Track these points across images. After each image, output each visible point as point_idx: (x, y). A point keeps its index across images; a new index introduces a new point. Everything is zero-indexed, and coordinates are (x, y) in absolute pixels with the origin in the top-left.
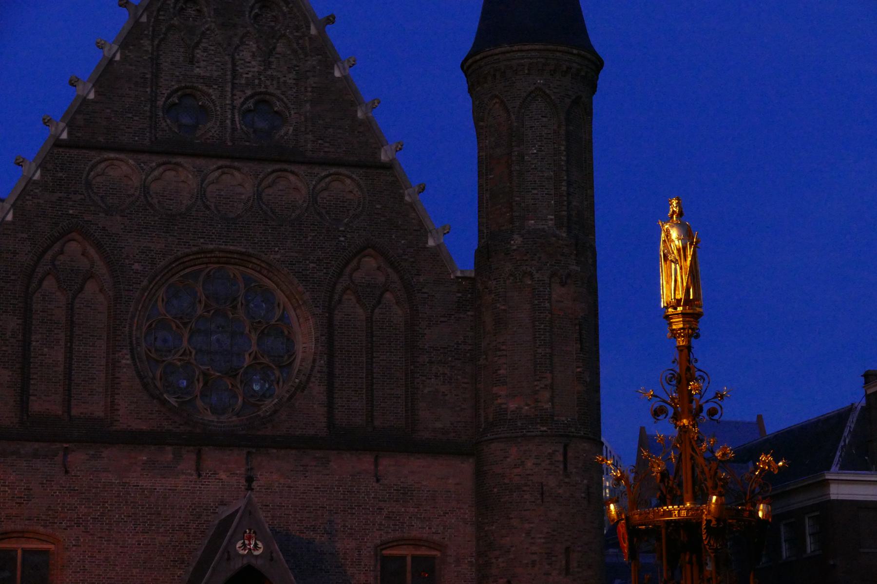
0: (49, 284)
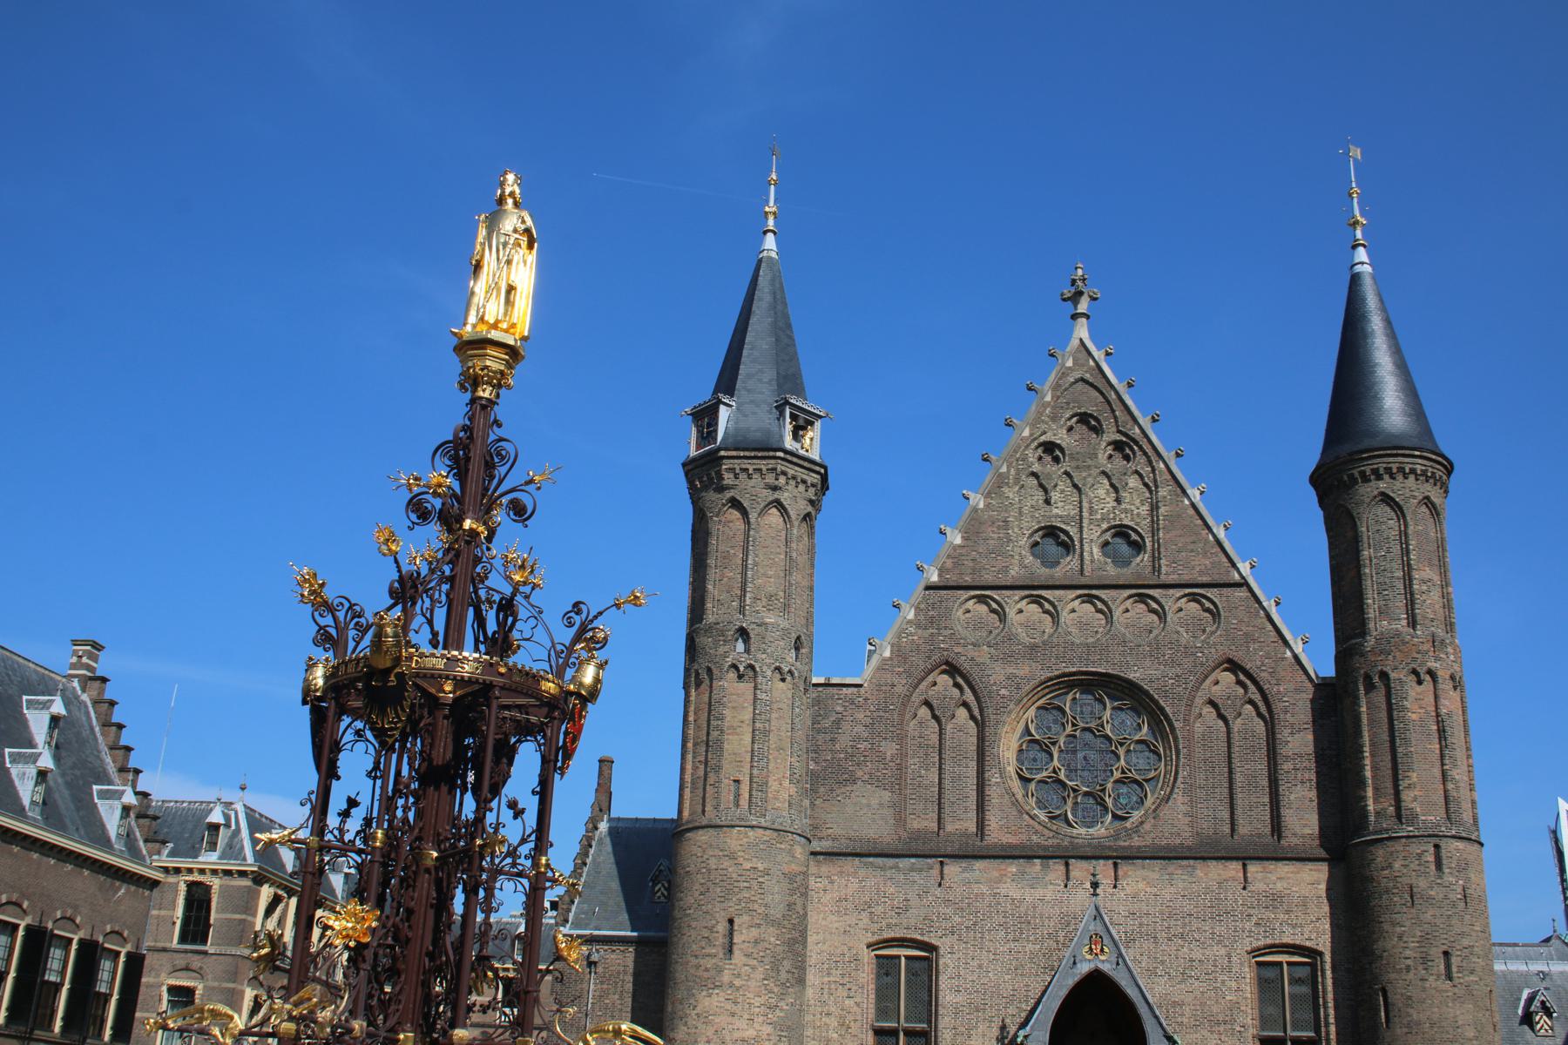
0: (924, 712)
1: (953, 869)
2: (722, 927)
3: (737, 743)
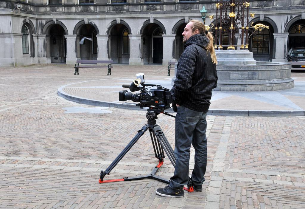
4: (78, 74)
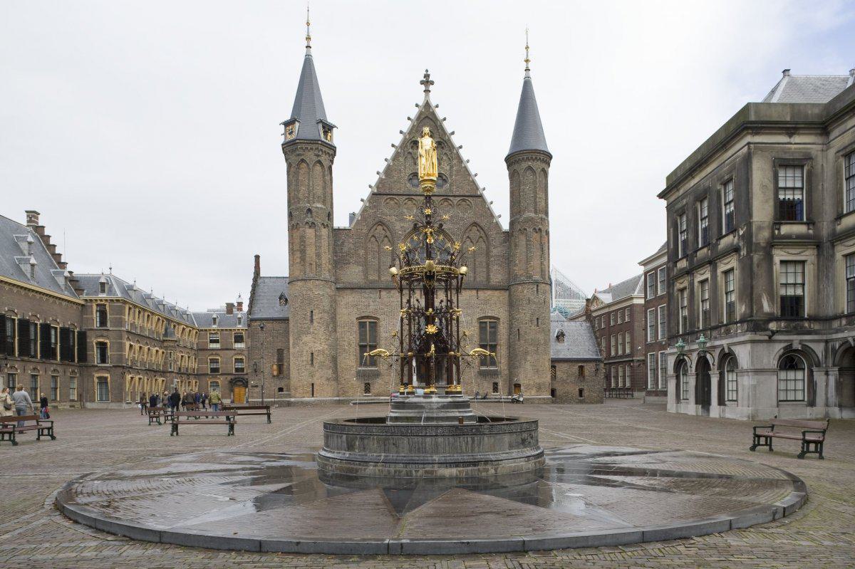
0: (373, 239)
1: (384, 293)
2: (309, 314)
3: (311, 252)
4: (177, 434)
